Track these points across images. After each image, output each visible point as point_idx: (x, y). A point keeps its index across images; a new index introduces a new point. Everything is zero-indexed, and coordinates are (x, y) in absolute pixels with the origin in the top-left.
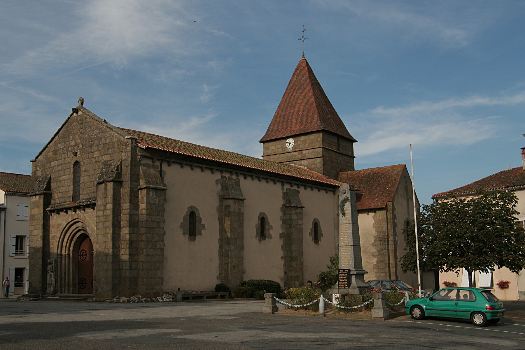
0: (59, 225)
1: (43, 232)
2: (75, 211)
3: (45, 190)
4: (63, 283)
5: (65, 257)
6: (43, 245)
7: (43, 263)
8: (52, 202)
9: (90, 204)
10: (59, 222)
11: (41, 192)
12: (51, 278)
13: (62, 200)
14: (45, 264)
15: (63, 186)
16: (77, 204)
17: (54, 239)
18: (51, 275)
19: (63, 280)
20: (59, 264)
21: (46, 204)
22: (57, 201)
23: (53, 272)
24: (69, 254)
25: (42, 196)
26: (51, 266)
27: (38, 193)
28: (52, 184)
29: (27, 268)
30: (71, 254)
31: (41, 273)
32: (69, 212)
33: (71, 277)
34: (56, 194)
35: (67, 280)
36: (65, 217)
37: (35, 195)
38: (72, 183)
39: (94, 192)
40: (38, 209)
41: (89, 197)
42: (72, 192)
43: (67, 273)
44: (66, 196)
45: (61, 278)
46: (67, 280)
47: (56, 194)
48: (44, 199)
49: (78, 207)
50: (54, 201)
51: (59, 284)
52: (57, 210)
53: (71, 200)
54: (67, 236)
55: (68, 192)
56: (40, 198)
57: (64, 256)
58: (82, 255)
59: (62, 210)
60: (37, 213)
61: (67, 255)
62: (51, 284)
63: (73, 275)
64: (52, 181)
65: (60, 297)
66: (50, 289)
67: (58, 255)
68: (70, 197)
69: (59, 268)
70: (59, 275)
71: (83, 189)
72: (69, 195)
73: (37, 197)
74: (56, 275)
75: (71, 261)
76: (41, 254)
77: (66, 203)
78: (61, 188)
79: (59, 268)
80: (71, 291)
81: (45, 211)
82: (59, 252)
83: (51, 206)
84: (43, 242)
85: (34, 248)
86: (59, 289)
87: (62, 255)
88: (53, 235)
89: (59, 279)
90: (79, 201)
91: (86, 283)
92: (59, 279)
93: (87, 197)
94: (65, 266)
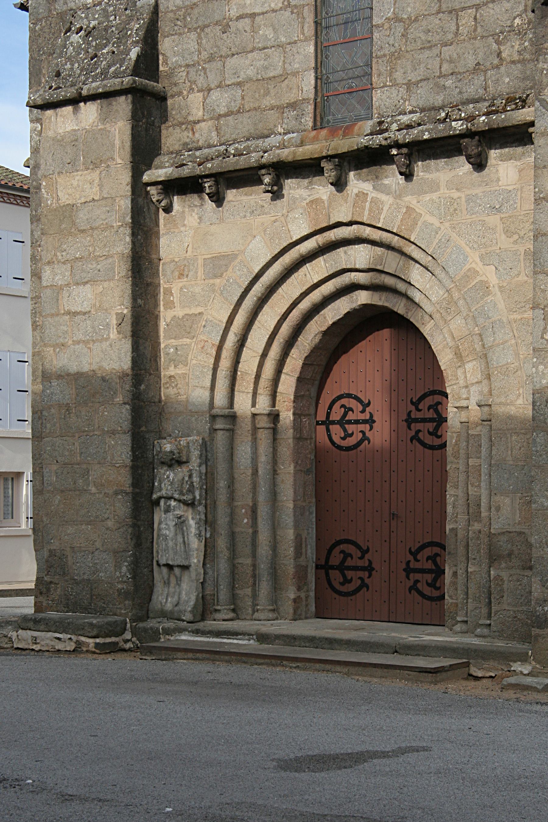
0: (218, 264)
1: (135, 297)
2: (339, 184)
3: (136, 71)
4: (245, 561)
5: (255, 429)
6: (134, 361)
7: (135, 458)
8: (171, 138)
9: (469, 134)
10: (217, 246)
11: (113, 84)
12: (178, 533)
13: (244, 125)
14: (144, 464)
15: (244, 52)
16: (364, 141)
17: (189, 334)
18: (181, 523)
19: (244, 548)
20: (221, 467)
21: (144, 150)
22: (205, 132)
23: (191, 504)
24: (274, 417)
25: (123, 105)
26: (181, 472)
27: (94, 86)
28: (166, 45)
29: (28, 475)
30: (287, 416)
31: (122, 508)
32: (293, 188)
33: (290, 534)
34: (196, 98)
35: (264, 550)
36: (266, 219)
37: (75, 101)
38: (309, 29)
39: (477, 68)
40: (95, 175)
41: (439, 100)
42: (310, 78)
43: (263, 511)
44: (268, 101)
45: (232, 535)
46: (264, 550)
47: (196, 98)
48: (136, 118)
49: (370, 158)
50: (186, 136)
51: (223, 566)
52: (216, 176)
53: (308, 121)
54: (268, 318)
55: (284, 76)
56: (104, 118)
57: (245, 426)
58: (342, 422)
59: (245, 178)
60: (93, 192)
61: (263, 422)
62: (185, 568)
63: (296, 526)
64: (164, 25)
65: (262, 638)
66: (177, 595)
67: (214, 417)
68: (293, 106)
69: (222, 484)
70: (222, 520)
71: (396, 56)
72: (291, 97)
73: (90, 112)
74: (209, 522)
75: (286, 449)
76: (125, 412)
77: (274, 140)
78: (232, 62)
79: (222, 484)
80: (288, 608)
81: (138, 188)
82: (220, 399)
83: (164, 159)
84: (135, 348)
85: (78, 375)
86: (224, 594)
87: (233, 418)
88: (179, 312)
89: (222, 543)
90: (368, 126)
91: (370, 569)
92: (222, 543)
93: (424, 96)
94: (255, 472)
